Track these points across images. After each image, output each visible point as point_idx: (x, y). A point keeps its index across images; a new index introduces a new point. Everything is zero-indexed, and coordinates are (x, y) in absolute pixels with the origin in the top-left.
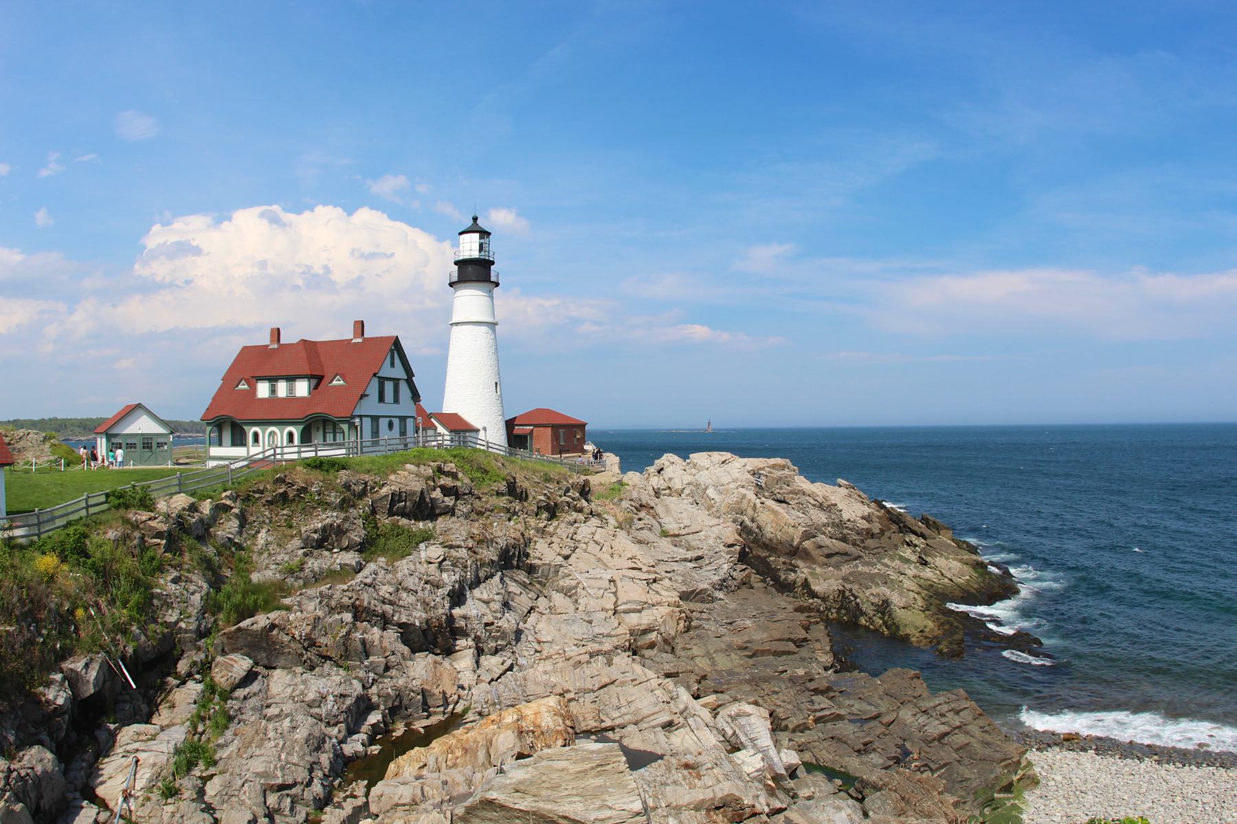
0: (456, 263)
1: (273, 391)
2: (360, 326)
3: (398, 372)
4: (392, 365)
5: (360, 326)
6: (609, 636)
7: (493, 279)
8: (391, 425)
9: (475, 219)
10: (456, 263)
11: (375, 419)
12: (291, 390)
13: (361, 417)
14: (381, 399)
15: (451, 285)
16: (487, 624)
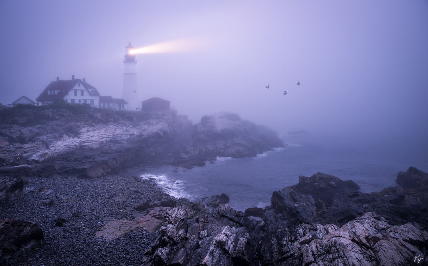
0: (125, 56)
1: (51, 93)
2: (73, 77)
3: (82, 87)
4: (79, 86)
5: (73, 77)
6: (73, 145)
7: (135, 61)
8: (80, 101)
9: (130, 43)
10: (125, 56)
11: (73, 100)
12: (54, 93)
13: (67, 99)
14: (76, 94)
15: (123, 62)
16: (42, 140)
